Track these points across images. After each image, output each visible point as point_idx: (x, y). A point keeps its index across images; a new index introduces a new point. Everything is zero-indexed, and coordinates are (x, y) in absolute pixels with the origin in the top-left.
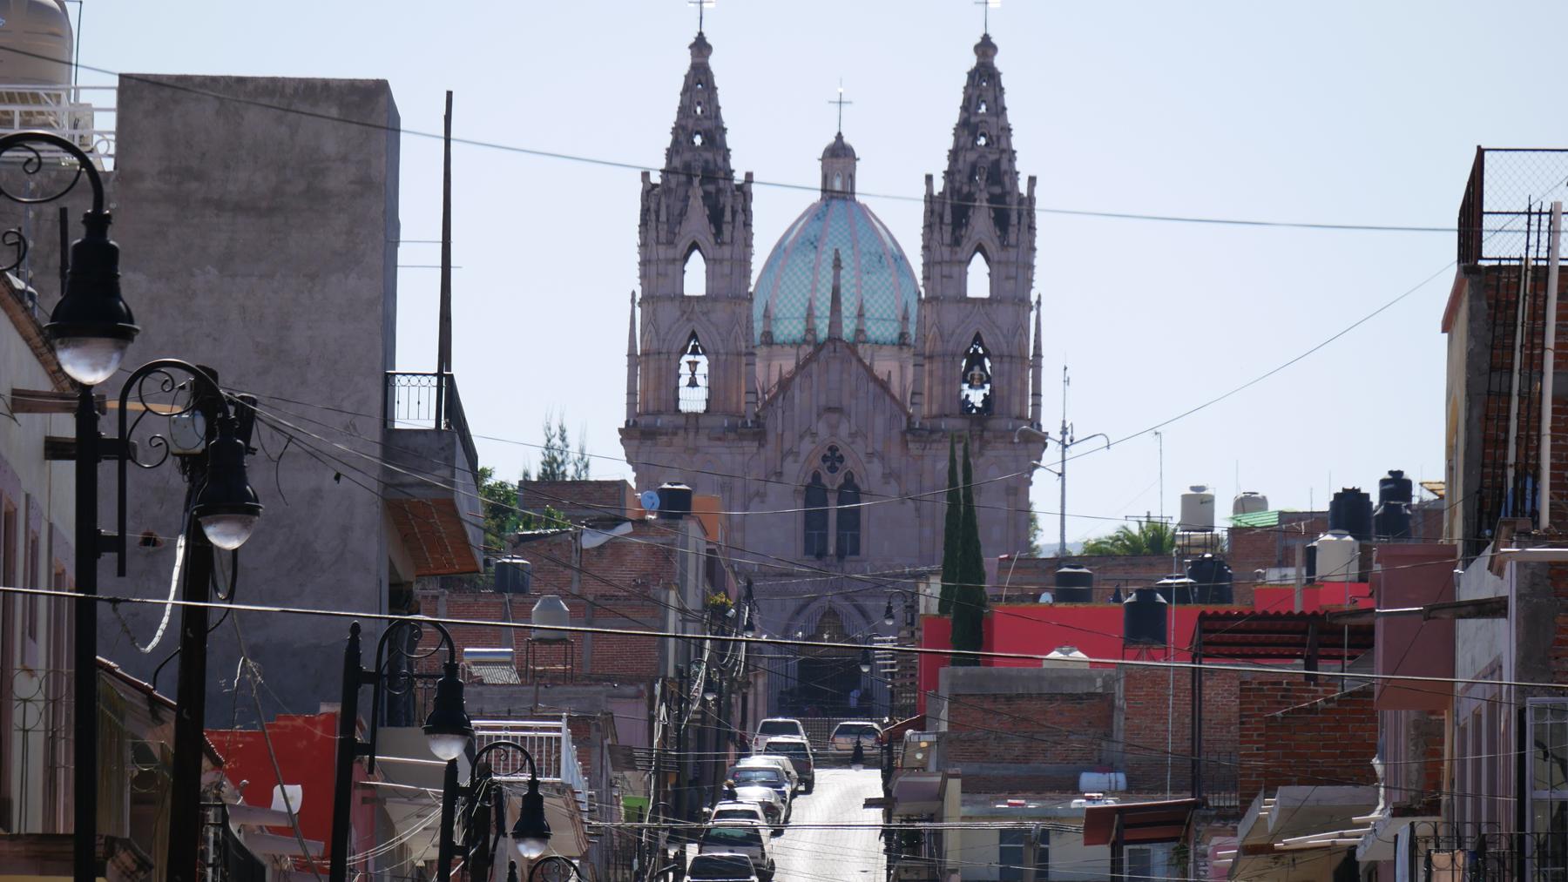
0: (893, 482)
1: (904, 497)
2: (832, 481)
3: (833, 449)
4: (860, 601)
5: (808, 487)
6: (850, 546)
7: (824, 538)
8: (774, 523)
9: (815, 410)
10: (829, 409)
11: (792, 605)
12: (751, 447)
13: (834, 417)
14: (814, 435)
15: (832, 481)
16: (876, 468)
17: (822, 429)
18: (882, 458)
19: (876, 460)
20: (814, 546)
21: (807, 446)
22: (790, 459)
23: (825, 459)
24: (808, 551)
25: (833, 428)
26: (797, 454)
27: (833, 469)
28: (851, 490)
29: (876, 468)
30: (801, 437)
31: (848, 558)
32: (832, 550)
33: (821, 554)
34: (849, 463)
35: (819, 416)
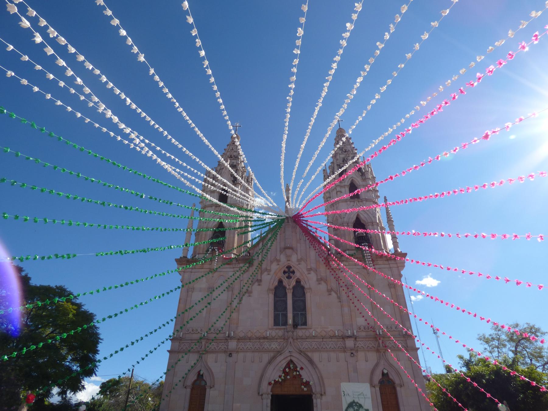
0: (323, 282)
1: (330, 291)
2: (289, 284)
3: (289, 267)
4: (309, 354)
5: (276, 288)
6: (301, 320)
7: (285, 316)
8: (256, 312)
10: (286, 248)
11: (266, 357)
13: (289, 252)
14: (278, 261)
15: (289, 284)
17: (283, 258)
18: (316, 271)
19: (312, 272)
20: (279, 319)
21: (274, 267)
22: (266, 273)
23: (285, 272)
24: (276, 323)
26: (270, 271)
27: (289, 277)
29: (313, 277)
30: (272, 262)
31: (299, 327)
32: (290, 321)
33: (285, 323)
34: (298, 275)
35: (281, 252)
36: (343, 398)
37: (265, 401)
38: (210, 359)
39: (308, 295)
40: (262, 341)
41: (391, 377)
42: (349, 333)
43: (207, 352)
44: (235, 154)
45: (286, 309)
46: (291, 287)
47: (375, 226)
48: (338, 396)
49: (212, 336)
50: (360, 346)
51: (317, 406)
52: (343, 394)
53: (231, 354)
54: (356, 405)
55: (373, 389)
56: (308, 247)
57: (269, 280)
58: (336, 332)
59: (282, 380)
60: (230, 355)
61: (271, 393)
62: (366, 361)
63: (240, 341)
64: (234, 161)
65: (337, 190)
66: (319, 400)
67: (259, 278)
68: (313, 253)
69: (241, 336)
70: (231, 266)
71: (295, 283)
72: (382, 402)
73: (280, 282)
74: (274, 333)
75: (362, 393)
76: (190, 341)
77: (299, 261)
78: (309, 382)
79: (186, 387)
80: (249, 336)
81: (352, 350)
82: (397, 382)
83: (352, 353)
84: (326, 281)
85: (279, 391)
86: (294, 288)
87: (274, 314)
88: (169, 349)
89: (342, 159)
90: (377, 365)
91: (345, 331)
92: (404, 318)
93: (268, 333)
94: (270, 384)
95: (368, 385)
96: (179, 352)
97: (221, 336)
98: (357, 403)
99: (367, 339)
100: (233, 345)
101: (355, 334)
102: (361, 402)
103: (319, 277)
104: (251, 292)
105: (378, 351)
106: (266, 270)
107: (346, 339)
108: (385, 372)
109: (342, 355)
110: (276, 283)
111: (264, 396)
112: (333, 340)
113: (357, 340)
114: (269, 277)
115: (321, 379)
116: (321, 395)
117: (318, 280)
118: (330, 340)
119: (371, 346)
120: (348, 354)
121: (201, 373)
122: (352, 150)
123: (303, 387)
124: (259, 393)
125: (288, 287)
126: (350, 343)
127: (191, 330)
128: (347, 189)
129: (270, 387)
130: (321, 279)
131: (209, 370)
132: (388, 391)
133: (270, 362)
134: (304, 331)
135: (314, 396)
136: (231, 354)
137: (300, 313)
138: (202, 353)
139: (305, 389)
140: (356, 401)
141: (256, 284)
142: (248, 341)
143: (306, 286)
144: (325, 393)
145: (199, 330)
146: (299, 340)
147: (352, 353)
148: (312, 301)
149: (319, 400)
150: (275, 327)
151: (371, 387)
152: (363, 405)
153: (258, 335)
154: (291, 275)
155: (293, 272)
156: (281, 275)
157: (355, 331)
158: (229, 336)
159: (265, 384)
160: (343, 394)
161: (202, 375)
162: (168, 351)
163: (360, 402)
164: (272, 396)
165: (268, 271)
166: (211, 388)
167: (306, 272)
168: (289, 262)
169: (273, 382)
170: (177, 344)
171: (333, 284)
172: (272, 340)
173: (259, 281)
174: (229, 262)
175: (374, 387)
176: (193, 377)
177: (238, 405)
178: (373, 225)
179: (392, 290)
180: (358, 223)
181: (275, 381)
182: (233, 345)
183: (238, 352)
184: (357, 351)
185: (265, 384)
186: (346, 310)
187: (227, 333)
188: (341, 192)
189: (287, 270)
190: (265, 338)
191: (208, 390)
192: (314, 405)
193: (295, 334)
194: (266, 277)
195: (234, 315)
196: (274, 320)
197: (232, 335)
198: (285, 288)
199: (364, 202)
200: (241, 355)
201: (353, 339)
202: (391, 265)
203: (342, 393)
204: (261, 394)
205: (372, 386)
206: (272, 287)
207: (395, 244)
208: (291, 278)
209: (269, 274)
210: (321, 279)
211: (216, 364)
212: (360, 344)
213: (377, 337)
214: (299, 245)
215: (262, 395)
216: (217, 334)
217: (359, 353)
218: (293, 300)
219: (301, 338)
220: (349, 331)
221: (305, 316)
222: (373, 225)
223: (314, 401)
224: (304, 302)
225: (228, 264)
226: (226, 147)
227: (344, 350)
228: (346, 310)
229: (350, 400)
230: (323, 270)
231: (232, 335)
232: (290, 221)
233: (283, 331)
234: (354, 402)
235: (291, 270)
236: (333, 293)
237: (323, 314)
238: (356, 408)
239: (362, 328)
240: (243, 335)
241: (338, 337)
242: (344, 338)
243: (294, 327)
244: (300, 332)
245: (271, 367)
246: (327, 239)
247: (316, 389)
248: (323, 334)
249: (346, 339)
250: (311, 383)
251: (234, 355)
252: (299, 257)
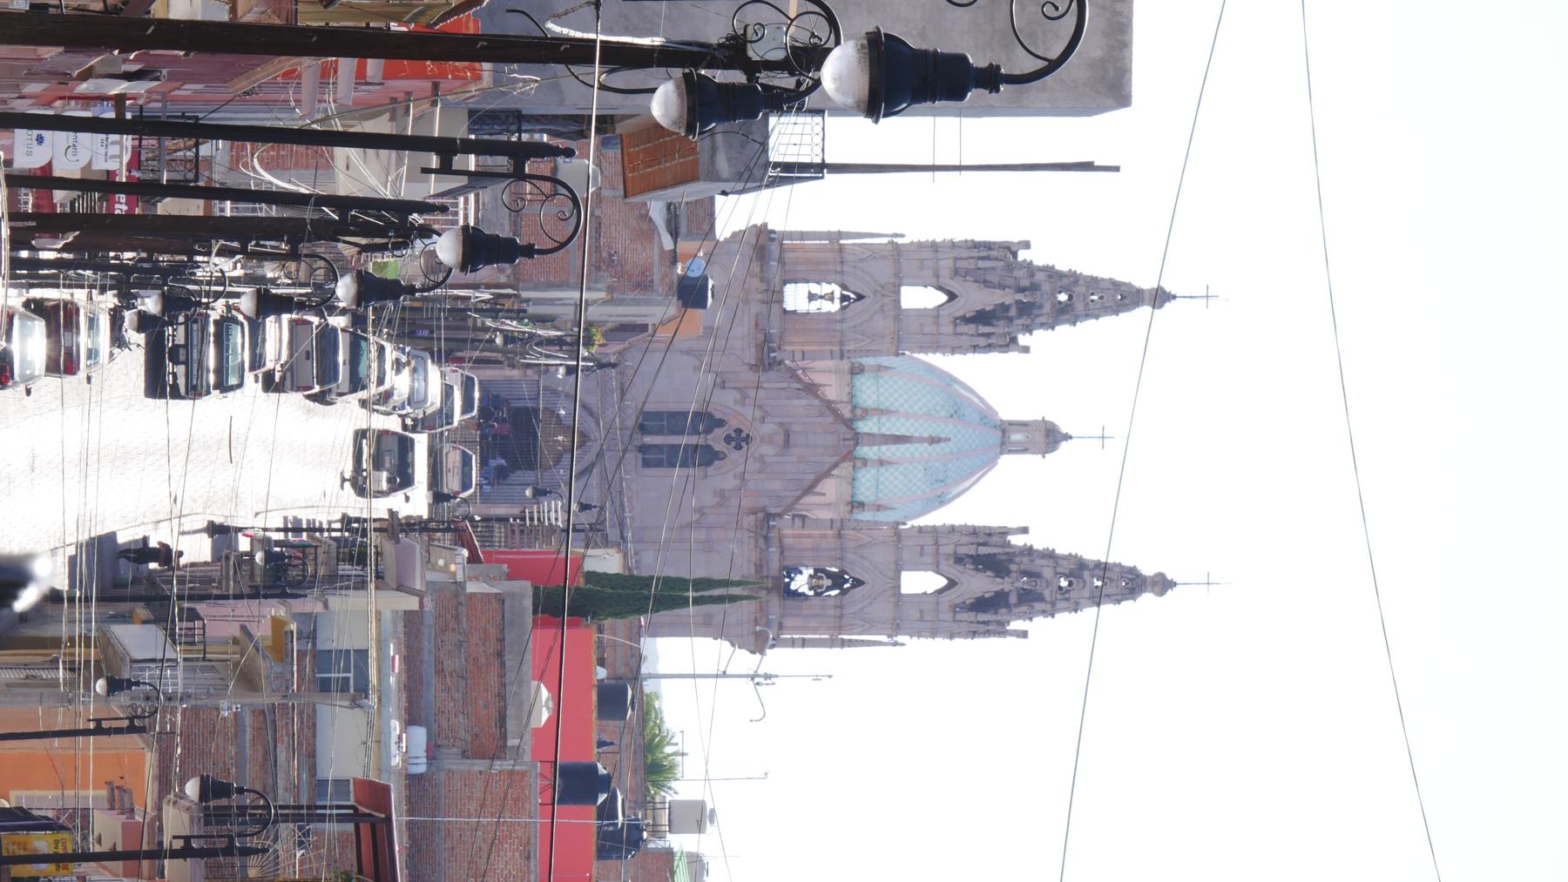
2: (716, 440)
5: (710, 415)
6: (654, 458)
7: (660, 432)
10: (787, 435)
13: (780, 439)
14: (763, 420)
15: (716, 440)
17: (768, 428)
22: (738, 396)
23: (738, 431)
24: (647, 415)
25: (767, 440)
27: (728, 439)
28: (708, 457)
29: (729, 483)
32: (648, 440)
34: (734, 455)
57: (725, 403)
86: (709, 447)
89: (1037, 570)
110: (718, 416)
117: (723, 491)
143: (710, 470)
156: (734, 423)
165: (743, 401)
188: (922, 554)
198: (708, 431)
221: (658, 464)
244: (633, 458)
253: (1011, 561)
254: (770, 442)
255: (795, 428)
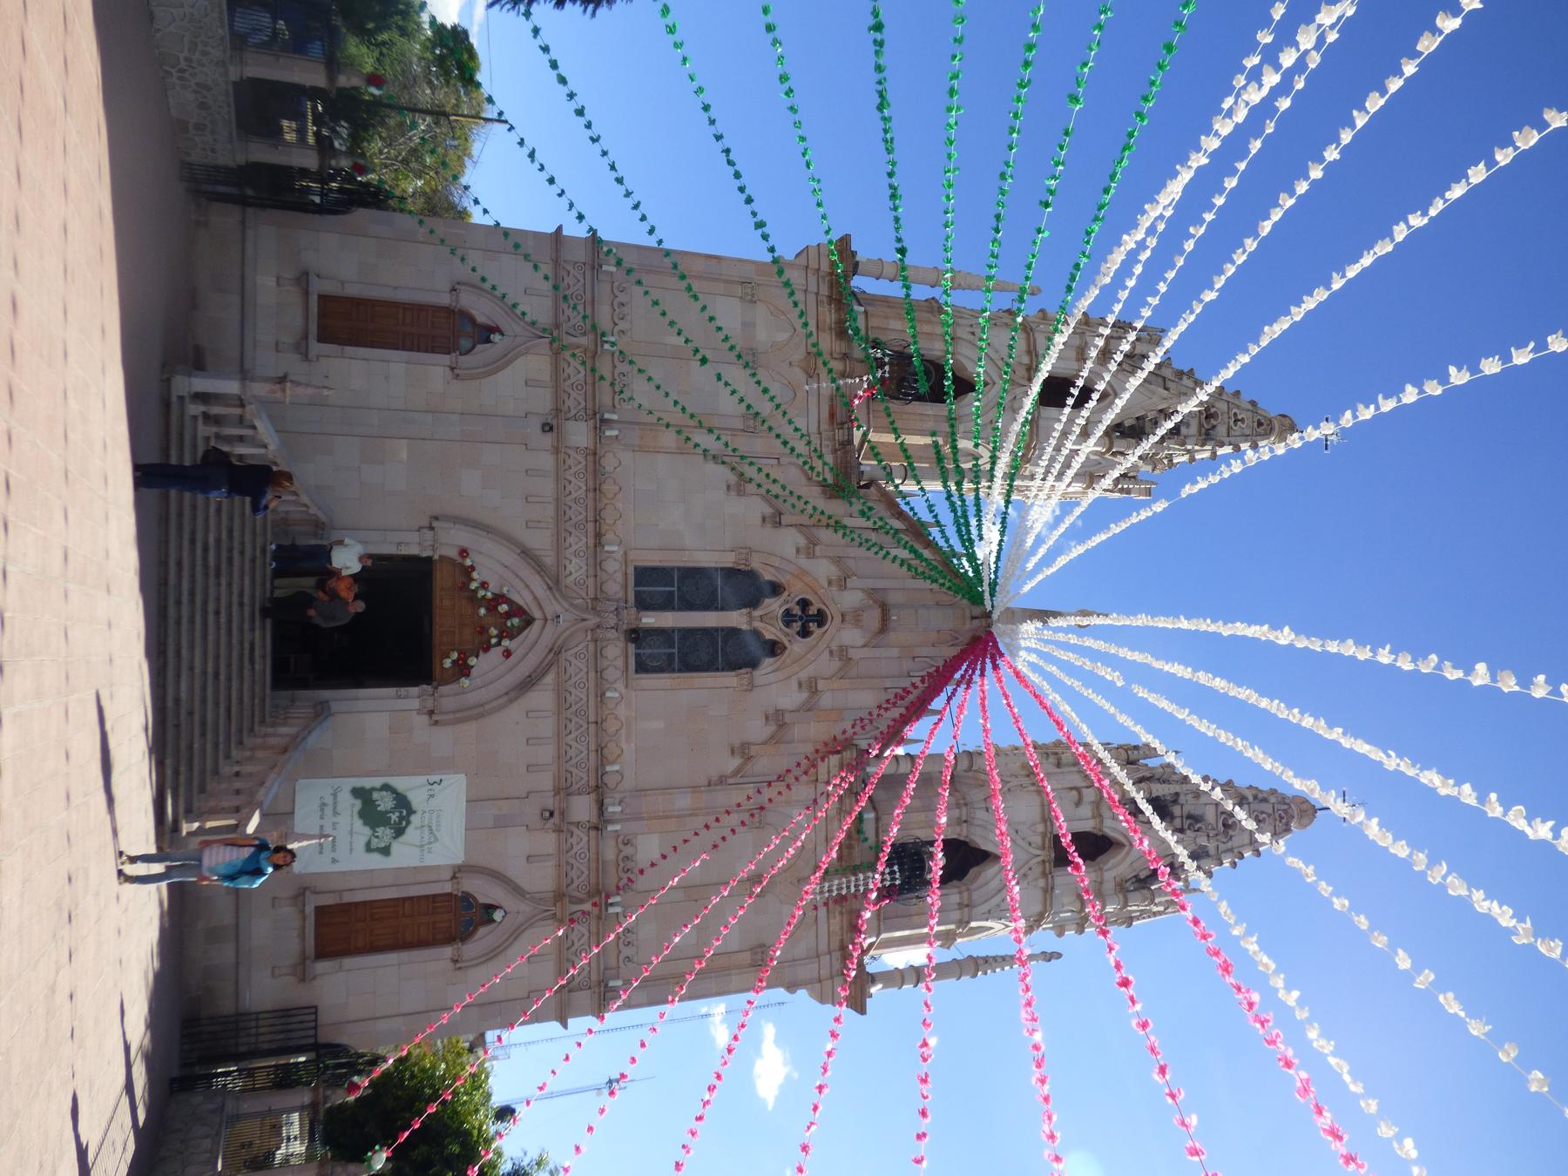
0: (772, 728)
1: (743, 750)
2: (767, 619)
3: (821, 618)
4: (549, 679)
5: (751, 575)
7: (666, 605)
8: (682, 513)
9: (879, 584)
10: (885, 610)
11: (540, 541)
12: (825, 471)
13: (873, 618)
14: (842, 583)
15: (767, 619)
16: (790, 698)
18: (808, 707)
19: (805, 695)
21: (823, 570)
22: (802, 541)
23: (804, 604)
24: (645, 575)
26: (810, 555)
29: (790, 698)
30: (837, 560)
31: (632, 648)
32: (650, 620)
33: (643, 604)
34: (797, 646)
35: (872, 593)
36: (422, 780)
37: (414, 537)
38: (537, 364)
39: (730, 679)
40: (590, 526)
41: (482, 931)
42: (613, 809)
43: (556, 354)
44: (1221, 430)
45: (689, 606)
46: (757, 624)
47: (956, 915)
48: (427, 764)
49: (604, 368)
50: (574, 840)
51: (399, 697)
52: (433, 778)
53: (551, 429)
54: (401, 818)
55: (448, 875)
56: (888, 683)
57: (778, 552)
58: (617, 767)
59: (475, 591)
60: (547, 428)
61: (436, 557)
62: (528, 858)
63: (590, 458)
64: (1194, 429)
65: (1084, 791)
66: (416, 703)
67: (785, 519)
68: (865, 699)
69: (604, 462)
70: (824, 426)
71: (768, 636)
72: (411, 899)
73: (776, 589)
74: (612, 566)
75: (436, 840)
76: (588, 295)
77: (842, 653)
78: (467, 675)
79: (454, 290)
80: (605, 487)
81: (562, 814)
82: (470, 949)
83: (552, 814)
84: (774, 740)
85: (442, 580)
87: (673, 569)
88: (565, 233)
89: (1197, 812)
90: (518, 891)
91: (618, 796)
92: (658, 990)
93: (615, 548)
94: (464, 553)
95: (459, 859)
96: (556, 262)
97: (605, 397)
98: (408, 823)
99: (593, 865)
100: (579, 434)
101: (610, 828)
102: (411, 834)
103: (788, 718)
104: (741, 493)
105: (559, 896)
106: (813, 542)
107: (593, 796)
108: (498, 915)
109: (546, 781)
111: (429, 535)
112: (593, 756)
113: (593, 833)
114: (790, 552)
115: (477, 713)
116: (431, 713)
117: (779, 713)
118: (593, 747)
119: (573, 874)
120: (550, 803)
121: (496, 337)
122: (1231, 850)
123: (455, 655)
124: (437, 518)
125: (757, 613)
126: (582, 808)
127: (622, 298)
128: (1087, 826)
129: (453, 553)
130: (782, 726)
131: (504, 361)
132: (444, 919)
133: (526, 553)
134: (620, 663)
135: (430, 688)
136: (551, 429)
137: (675, 651)
138: (553, 336)
139: (448, 663)
140: (413, 818)
141: (768, 511)
142: (591, 484)
144: (436, 723)
145: (622, 325)
146: (591, 647)
147: (552, 814)
148: (710, 690)
149: (416, 703)
150: (631, 571)
151: (454, 866)
152: (401, 839)
153: (608, 516)
154: (797, 626)
155: (805, 633)
156: (797, 590)
157: (618, 827)
158: (603, 421)
159: (463, 537)
160: (433, 778)
161: (488, 341)
162: (560, 228)
163: (410, 831)
164: (429, 560)
165: (810, 550)
166: (452, 369)
167: (804, 675)
168: (838, 618)
169: (468, 562)
170: (581, 255)
171: (766, 764)
172: (591, 561)
173: (776, 520)
174: (840, 416)
175: (454, 877)
176: (482, 310)
177: (404, 456)
178: (961, 906)
179: (746, 957)
180: (965, 859)
181: (473, 568)
182: (579, 434)
183: (556, 450)
184: (559, 830)
185: (463, 537)
186: (683, 802)
187: (615, 417)
188: (1078, 803)
189: (813, 610)
190: (598, 535)
191: (445, 359)
192: (403, 691)
193: (612, 634)
194: (788, 541)
195: (669, 439)
196: (654, 569)
197: (608, 433)
198: (753, 603)
199: (1042, 883)
200: (547, 461)
201: (594, 820)
202: (825, 959)
203: (436, 778)
204: (435, 524)
205: (457, 872)
206: (755, 564)
207: (896, 978)
208: (788, 624)
209: (798, 551)
210: (782, 726)
211: (519, 382)
212: (581, 840)
213: (599, 895)
214: (895, 652)
215: (431, 528)
216: (612, 384)
217: (553, 836)
218: (716, 629)
219: (598, 654)
220: (618, 809)
221: (666, 667)
222: (961, 906)
223: (414, 690)
224: (709, 666)
225: (832, 415)
226: (1246, 397)
227: (563, 790)
228: (683, 802)
229: (416, 798)
230: (810, 733)
231: (608, 433)
232: (976, 623)
233: (621, 594)
234: (411, 812)
235: (813, 626)
236: (735, 762)
237: (671, 725)
238: (394, 817)
239: (627, 851)
240: (609, 468)
241: (600, 772)
242: (599, 791)
243: (634, 631)
244: (616, 651)
245: (510, 557)
246: (915, 749)
247: (449, 696)
248: (611, 726)
249: (593, 796)
250: (465, 682)
251: (548, 440)
252: (852, 653)
253: (1175, 802)
254: (857, 621)
255: (894, 598)
